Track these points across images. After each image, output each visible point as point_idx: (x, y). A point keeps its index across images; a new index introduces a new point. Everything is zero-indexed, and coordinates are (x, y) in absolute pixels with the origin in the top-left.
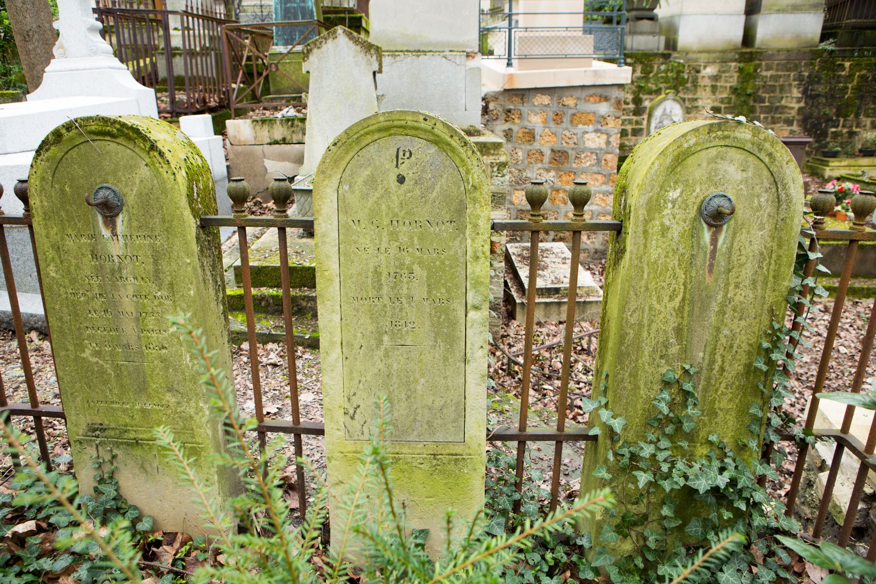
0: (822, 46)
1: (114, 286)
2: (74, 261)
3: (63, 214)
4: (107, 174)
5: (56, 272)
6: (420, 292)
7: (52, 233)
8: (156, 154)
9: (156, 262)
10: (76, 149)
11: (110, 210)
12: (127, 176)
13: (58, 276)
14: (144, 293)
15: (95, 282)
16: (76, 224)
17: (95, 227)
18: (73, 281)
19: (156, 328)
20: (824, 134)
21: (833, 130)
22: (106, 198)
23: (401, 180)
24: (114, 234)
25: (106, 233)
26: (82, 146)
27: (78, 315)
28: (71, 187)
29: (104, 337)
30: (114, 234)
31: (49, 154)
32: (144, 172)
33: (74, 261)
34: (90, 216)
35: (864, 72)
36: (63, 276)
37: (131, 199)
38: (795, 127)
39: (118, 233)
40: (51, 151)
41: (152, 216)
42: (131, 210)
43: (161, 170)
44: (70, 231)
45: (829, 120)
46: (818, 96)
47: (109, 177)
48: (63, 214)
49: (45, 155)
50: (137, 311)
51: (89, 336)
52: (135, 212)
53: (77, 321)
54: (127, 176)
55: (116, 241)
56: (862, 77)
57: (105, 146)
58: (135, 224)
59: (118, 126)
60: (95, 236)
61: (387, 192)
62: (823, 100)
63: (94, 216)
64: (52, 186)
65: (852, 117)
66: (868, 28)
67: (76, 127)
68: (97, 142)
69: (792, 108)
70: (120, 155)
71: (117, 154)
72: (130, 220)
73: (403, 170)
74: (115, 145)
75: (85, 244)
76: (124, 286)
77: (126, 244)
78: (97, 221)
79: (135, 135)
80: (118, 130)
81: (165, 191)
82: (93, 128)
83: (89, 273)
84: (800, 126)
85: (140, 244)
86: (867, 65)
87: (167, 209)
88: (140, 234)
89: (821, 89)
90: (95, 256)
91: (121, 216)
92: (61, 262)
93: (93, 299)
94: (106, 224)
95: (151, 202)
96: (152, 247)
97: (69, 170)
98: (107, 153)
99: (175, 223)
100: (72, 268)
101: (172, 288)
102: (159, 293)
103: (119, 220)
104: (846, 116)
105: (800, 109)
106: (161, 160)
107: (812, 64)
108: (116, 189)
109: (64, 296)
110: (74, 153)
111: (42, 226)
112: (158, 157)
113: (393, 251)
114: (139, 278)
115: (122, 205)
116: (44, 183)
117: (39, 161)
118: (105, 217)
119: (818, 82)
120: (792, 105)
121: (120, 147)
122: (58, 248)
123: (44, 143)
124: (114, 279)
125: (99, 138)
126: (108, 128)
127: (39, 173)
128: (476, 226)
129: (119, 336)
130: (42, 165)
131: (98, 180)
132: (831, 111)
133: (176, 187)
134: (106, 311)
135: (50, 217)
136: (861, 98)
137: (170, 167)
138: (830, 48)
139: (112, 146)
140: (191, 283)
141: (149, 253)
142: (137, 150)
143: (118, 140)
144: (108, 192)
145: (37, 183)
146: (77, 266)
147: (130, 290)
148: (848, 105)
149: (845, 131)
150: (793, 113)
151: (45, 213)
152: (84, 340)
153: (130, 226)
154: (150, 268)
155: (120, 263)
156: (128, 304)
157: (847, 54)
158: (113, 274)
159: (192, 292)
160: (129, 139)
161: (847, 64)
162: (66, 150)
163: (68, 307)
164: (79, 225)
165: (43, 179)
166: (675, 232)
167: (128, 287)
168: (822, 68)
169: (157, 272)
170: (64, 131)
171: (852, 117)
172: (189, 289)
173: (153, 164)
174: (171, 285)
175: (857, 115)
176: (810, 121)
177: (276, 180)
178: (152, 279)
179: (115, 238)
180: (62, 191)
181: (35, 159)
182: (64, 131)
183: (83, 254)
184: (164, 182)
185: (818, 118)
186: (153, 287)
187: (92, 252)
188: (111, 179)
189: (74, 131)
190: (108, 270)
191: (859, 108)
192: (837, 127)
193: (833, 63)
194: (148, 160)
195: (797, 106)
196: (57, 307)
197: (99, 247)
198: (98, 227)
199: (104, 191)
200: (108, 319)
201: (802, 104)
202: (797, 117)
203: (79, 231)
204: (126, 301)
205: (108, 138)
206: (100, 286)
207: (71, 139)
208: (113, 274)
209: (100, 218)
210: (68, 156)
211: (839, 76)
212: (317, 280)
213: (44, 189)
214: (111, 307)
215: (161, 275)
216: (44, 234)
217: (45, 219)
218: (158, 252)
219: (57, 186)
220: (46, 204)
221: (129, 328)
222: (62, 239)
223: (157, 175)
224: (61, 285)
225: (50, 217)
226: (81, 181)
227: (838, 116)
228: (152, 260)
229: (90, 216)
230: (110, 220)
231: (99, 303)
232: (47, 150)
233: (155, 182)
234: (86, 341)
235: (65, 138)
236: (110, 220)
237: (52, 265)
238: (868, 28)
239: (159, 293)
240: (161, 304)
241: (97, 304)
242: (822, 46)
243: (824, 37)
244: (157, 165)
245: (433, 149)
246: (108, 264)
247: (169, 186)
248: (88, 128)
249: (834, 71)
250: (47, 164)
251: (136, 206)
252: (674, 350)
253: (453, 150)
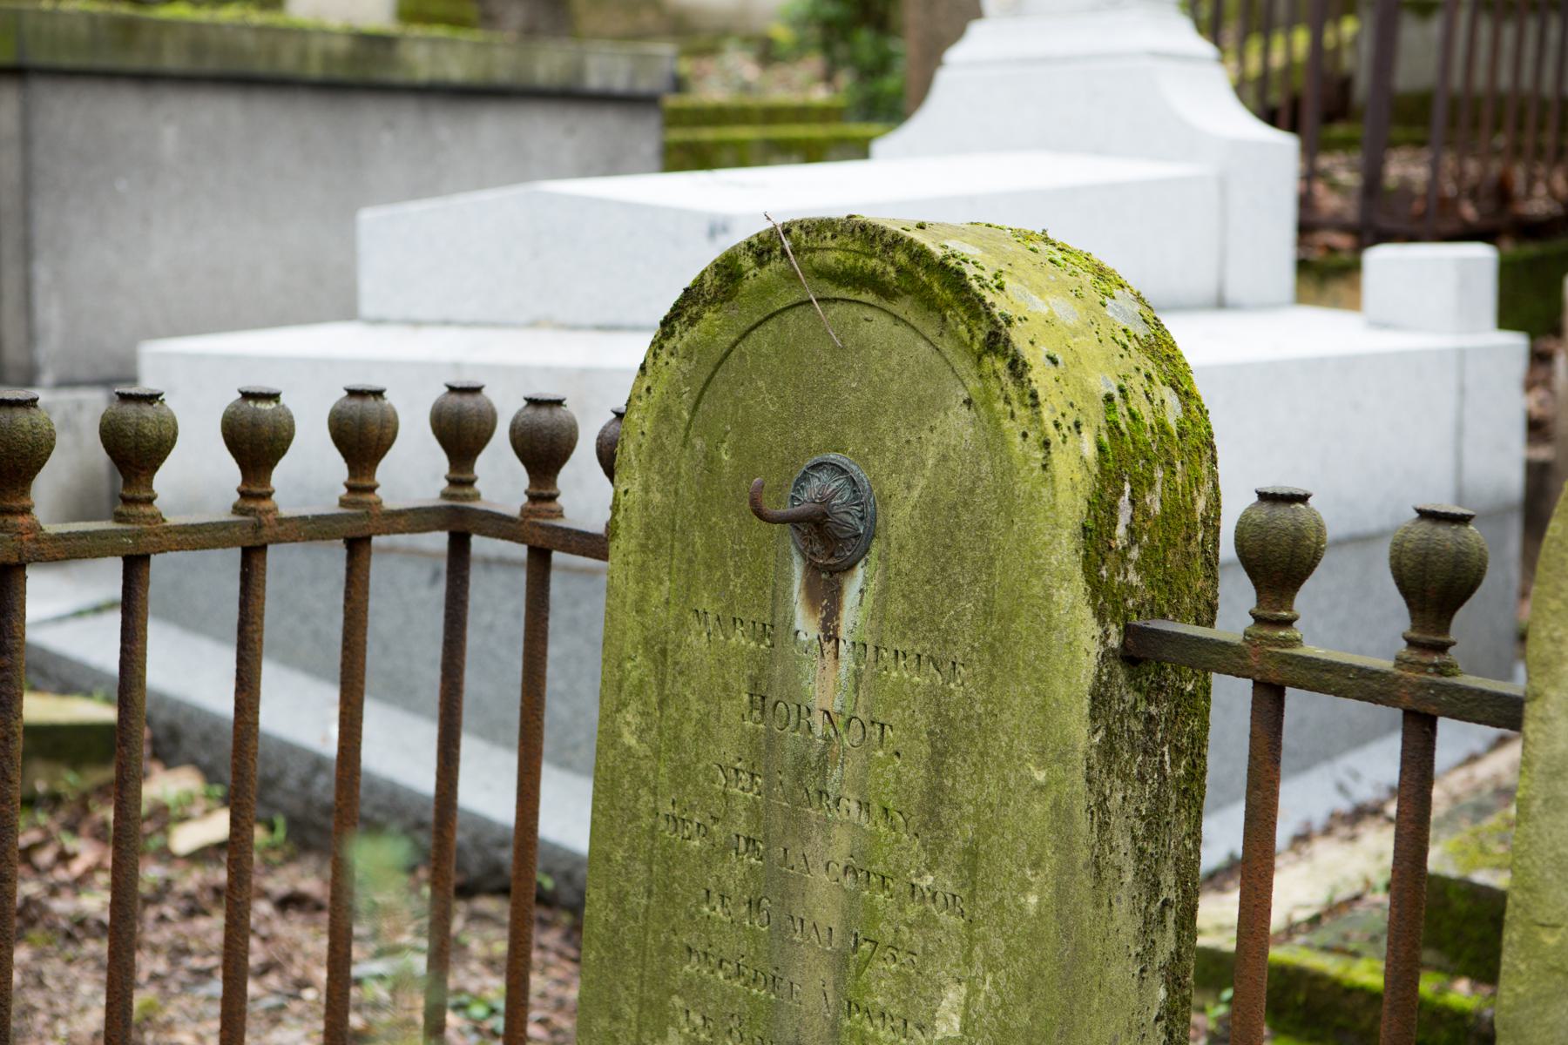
1: (797, 824)
2: (696, 706)
3: (698, 539)
5: (641, 733)
7: (657, 596)
8: (1001, 366)
9: (937, 760)
10: (771, 325)
11: (831, 543)
12: (904, 434)
13: (642, 749)
14: (879, 867)
15: (743, 792)
16: (726, 576)
17: (779, 598)
18: (682, 775)
19: (896, 1010)
22: (825, 501)
24: (830, 634)
25: (806, 624)
26: (790, 317)
27: (670, 898)
28: (736, 451)
29: (732, 1000)
30: (830, 634)
32: (957, 425)
33: (696, 706)
34: (771, 558)
36: (657, 752)
37: (901, 518)
39: (842, 634)
40: (702, 324)
41: (954, 590)
42: (894, 555)
43: (1007, 423)
44: (705, 601)
47: (850, 432)
48: (698, 539)
49: (686, 336)
50: (847, 930)
51: (689, 983)
52: (906, 566)
53: (667, 919)
54: (904, 434)
55: (829, 657)
57: (856, 321)
58: (898, 607)
59: (902, 258)
60: (772, 630)
63: (783, 560)
64: (685, 442)
67: (784, 253)
68: (837, 309)
70: (895, 358)
71: (886, 353)
72: (885, 590)
74: (883, 321)
75: (738, 651)
76: (826, 825)
77: (857, 675)
78: (788, 580)
79: (948, 295)
80: (900, 270)
81: (1007, 504)
82: (831, 258)
83: (730, 758)
85: (900, 683)
87: (1005, 571)
88: (907, 646)
90: (760, 700)
91: (859, 572)
92: (662, 703)
93: (725, 851)
95: (960, 536)
96: (936, 699)
97: (740, 393)
98: (860, 347)
99: (1020, 625)
100: (689, 729)
101: (974, 870)
102: (929, 879)
103: (854, 585)
106: (1012, 390)
108: (862, 475)
109: (646, 821)
110: (763, 339)
111: (632, 570)
112: (1006, 378)
114: (875, 805)
115: (871, 535)
116: (665, 428)
117: (664, 355)
118: (813, 569)
121: (899, 330)
122: (664, 652)
123: (690, 295)
124: (800, 793)
125: (842, 293)
126: (874, 262)
127: (655, 393)
129: (775, 1006)
130: (672, 366)
131: (817, 439)
133: (1046, 492)
134: (754, 905)
135: (659, 545)
137: (1037, 419)
139: (876, 327)
140: (1036, 865)
141: (922, 721)
142: (947, 346)
143: (901, 307)
145: (647, 426)
146: (703, 724)
147: (841, 847)
151: (648, 529)
152: (672, 992)
153: (880, 613)
154: (916, 775)
155: (827, 739)
156: (823, 897)
158: (799, 777)
159: (1033, 900)
160: (930, 304)
162: (744, 325)
163: (649, 863)
164: (736, 584)
165: (665, 414)
167: (837, 832)
169: (936, 796)
170: (747, 262)
172: (1025, 886)
173: (988, 403)
174: (972, 854)
177: (1424, 515)
178: (915, 820)
179: (829, 647)
180: (711, 460)
181: (657, 345)
182: (747, 262)
183: (726, 687)
184: (1010, 471)
186: (914, 851)
187: (755, 683)
188: (853, 437)
189: (776, 265)
190: (789, 760)
194: (974, 385)
196: (619, 855)
197: (778, 670)
198: (788, 602)
199: (824, 476)
200: (755, 936)
203: (730, 607)
204: (821, 880)
205: (868, 297)
206: (753, 809)
207: (765, 291)
208: (799, 777)
210: (747, 346)
212: (1506, 958)
213: (662, 447)
214: (773, 893)
215: (945, 812)
216: (631, 598)
217: (643, 548)
218: (950, 722)
219: (698, 443)
220: (657, 497)
221: (812, 985)
222: (681, 624)
223: (995, 440)
224: (645, 782)
225: (659, 545)
226: (768, 435)
228: (925, 749)
229: (771, 558)
230: (825, 588)
231: (739, 871)
232: (692, 322)
233: (985, 466)
234: (677, 1001)
235: (746, 286)
236: (825, 588)
237: (635, 705)
239: (929, 879)
240: (926, 922)
241: (735, 870)
244: (1000, 405)
246: (792, 738)
247: (1022, 488)
248: (817, 258)
250: (685, 367)
251: (911, 544)
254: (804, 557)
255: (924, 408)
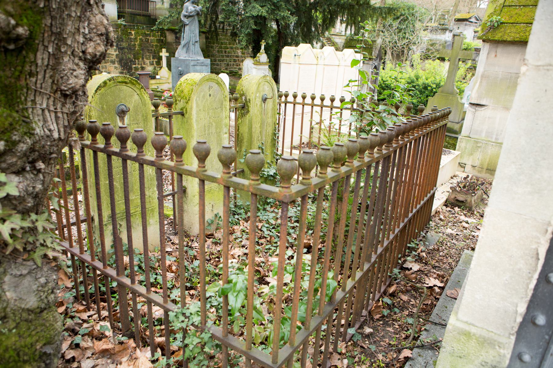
0: (119, 22)
3: (102, 118)
4: (122, 99)
6: (214, 131)
20: (131, 68)
21: (134, 66)
23: (210, 95)
28: (106, 106)
31: (101, 91)
32: (136, 97)
35: (141, 37)
38: (116, 65)
45: (131, 61)
46: (124, 48)
49: (99, 92)
56: (141, 39)
58: (132, 119)
61: (207, 100)
62: (126, 50)
65: (141, 59)
66: (139, 15)
69: (113, 55)
73: (211, 92)
82: (120, 80)
84: (119, 64)
86: (142, 33)
89: (124, 45)
94: (120, 121)
104: (138, 59)
105: (117, 55)
107: (117, 31)
110: (108, 91)
113: (208, 118)
119: (122, 41)
120: (112, 53)
123: (99, 87)
128: (226, 108)
132: (131, 57)
136: (143, 50)
138: (124, 23)
139: (124, 87)
144: (123, 106)
148: (138, 54)
149: (139, 66)
150: (114, 57)
153: (130, 120)
157: (132, 27)
161: (133, 32)
166: (258, 105)
168: (122, 34)
170: (108, 82)
171: (141, 59)
175: (143, 59)
176: (123, 61)
180: (102, 108)
182: (108, 82)
184: (145, 101)
185: (126, 60)
188: (123, 101)
189: (112, 81)
191: (143, 55)
192: (135, 64)
193: (127, 31)
194: (138, 92)
195: (115, 53)
201: (117, 53)
202: (116, 60)
207: (110, 85)
209: (118, 118)
211: (131, 38)
227: (135, 59)
238: (139, 15)
242: (119, 22)
243: (119, 17)
245: (217, 85)
247: (147, 102)
249: (128, 35)
252: (260, 138)
253: (221, 85)
254: (119, 116)
255: (131, 96)
